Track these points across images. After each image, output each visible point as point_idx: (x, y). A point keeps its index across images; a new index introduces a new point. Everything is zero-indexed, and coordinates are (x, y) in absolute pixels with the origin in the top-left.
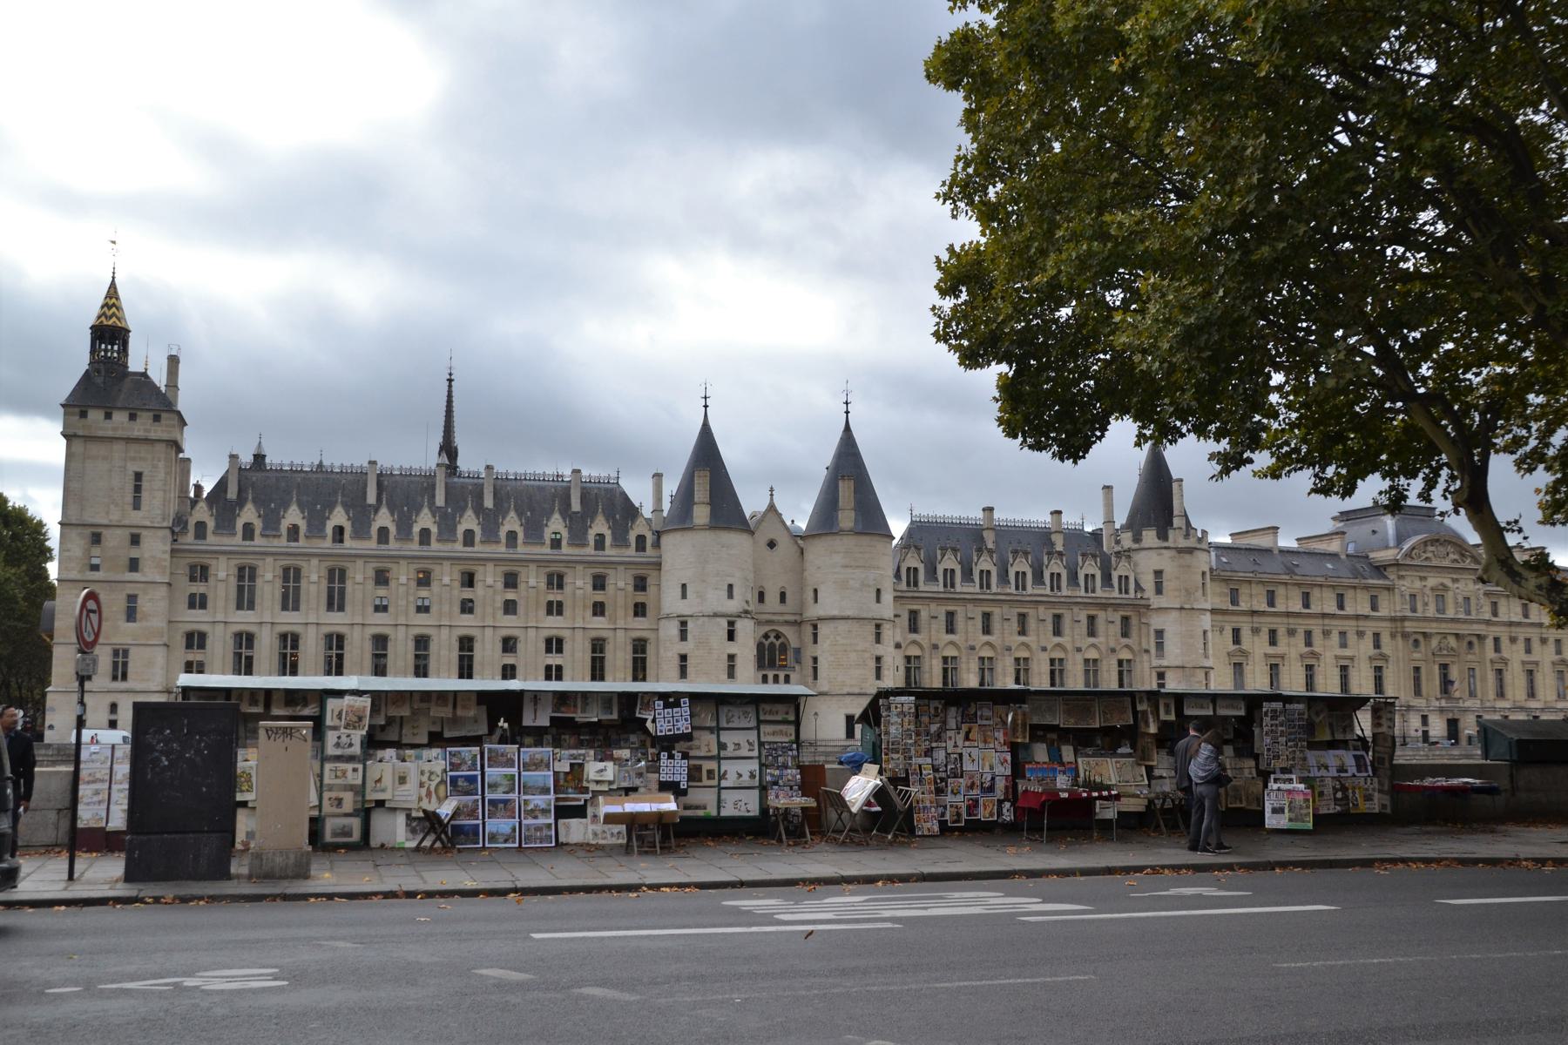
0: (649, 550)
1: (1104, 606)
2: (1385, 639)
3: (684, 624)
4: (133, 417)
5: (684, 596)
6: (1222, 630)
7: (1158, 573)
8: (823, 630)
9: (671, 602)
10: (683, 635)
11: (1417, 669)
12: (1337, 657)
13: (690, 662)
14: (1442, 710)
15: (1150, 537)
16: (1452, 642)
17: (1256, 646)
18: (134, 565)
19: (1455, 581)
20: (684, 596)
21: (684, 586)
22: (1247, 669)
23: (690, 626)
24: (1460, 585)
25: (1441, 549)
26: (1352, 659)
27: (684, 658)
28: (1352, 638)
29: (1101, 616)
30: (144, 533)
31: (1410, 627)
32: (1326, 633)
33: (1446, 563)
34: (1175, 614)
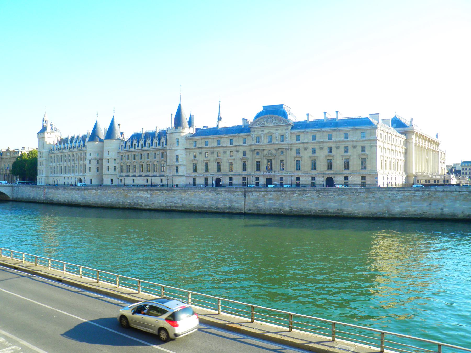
2: (248, 153)
6: (190, 154)
11: (258, 162)
12: (228, 160)
14: (264, 175)
16: (274, 152)
17: (201, 158)
19: (277, 130)
22: (197, 165)
24: (279, 132)
25: (269, 120)
26: (234, 159)
28: (235, 153)
29: (157, 152)
32: (225, 152)
33: (272, 124)
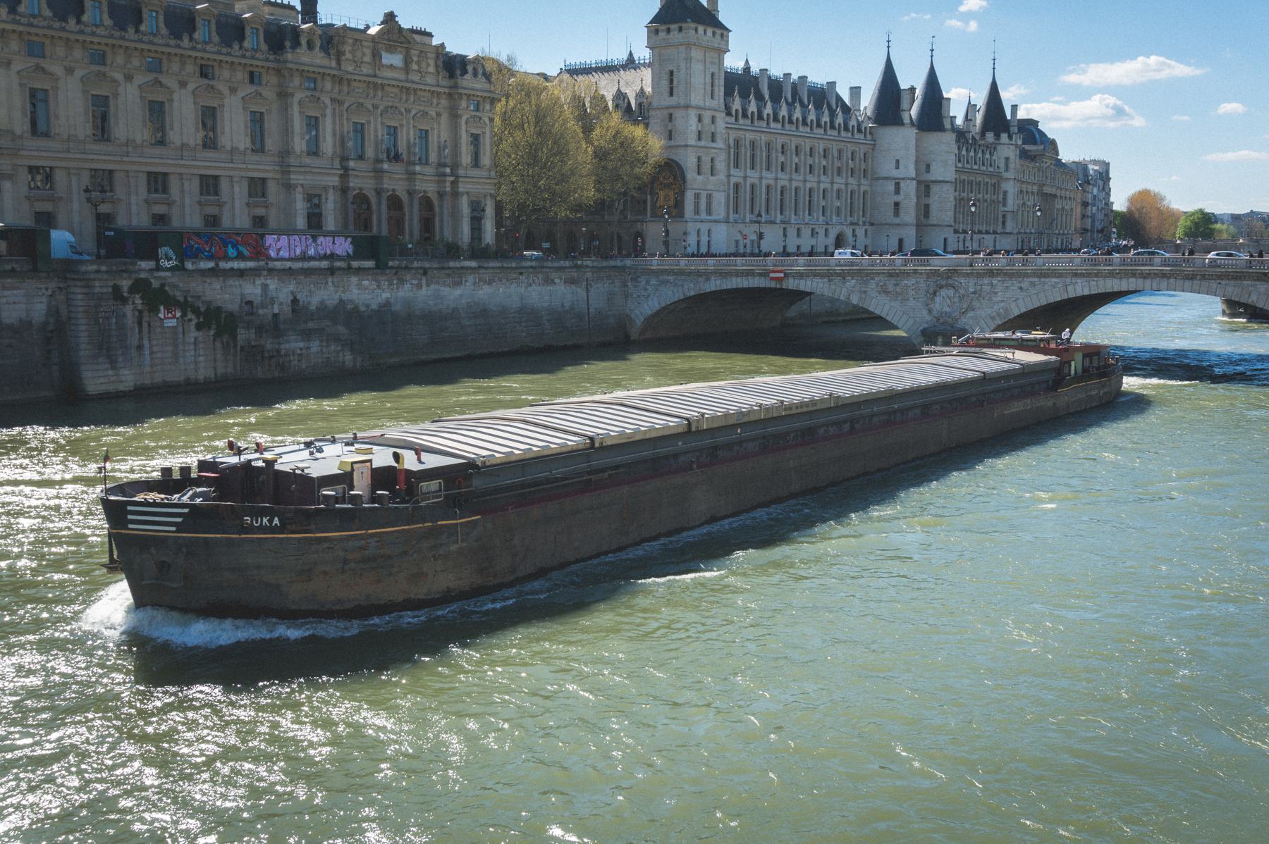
0: (869, 137)
1: (991, 175)
3: (897, 185)
4: (714, 33)
5: (897, 168)
7: (1007, 159)
8: (935, 189)
9: (887, 169)
10: (897, 191)
13: (902, 206)
15: (1004, 137)
18: (713, 138)
20: (897, 168)
21: (898, 161)
23: (902, 185)
27: (897, 204)
30: (717, 115)
31: (1047, 190)
34: (1012, 183)
